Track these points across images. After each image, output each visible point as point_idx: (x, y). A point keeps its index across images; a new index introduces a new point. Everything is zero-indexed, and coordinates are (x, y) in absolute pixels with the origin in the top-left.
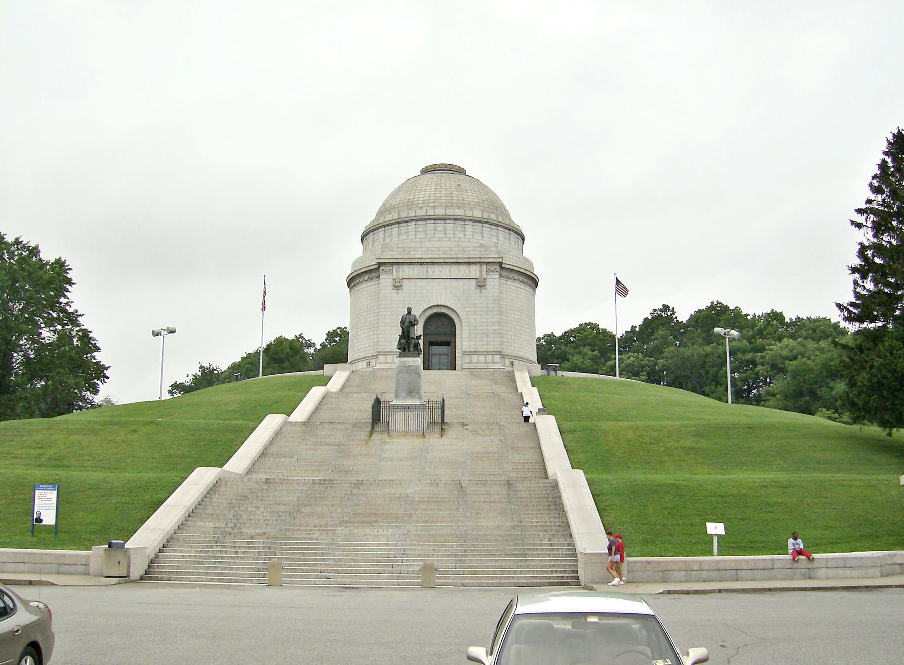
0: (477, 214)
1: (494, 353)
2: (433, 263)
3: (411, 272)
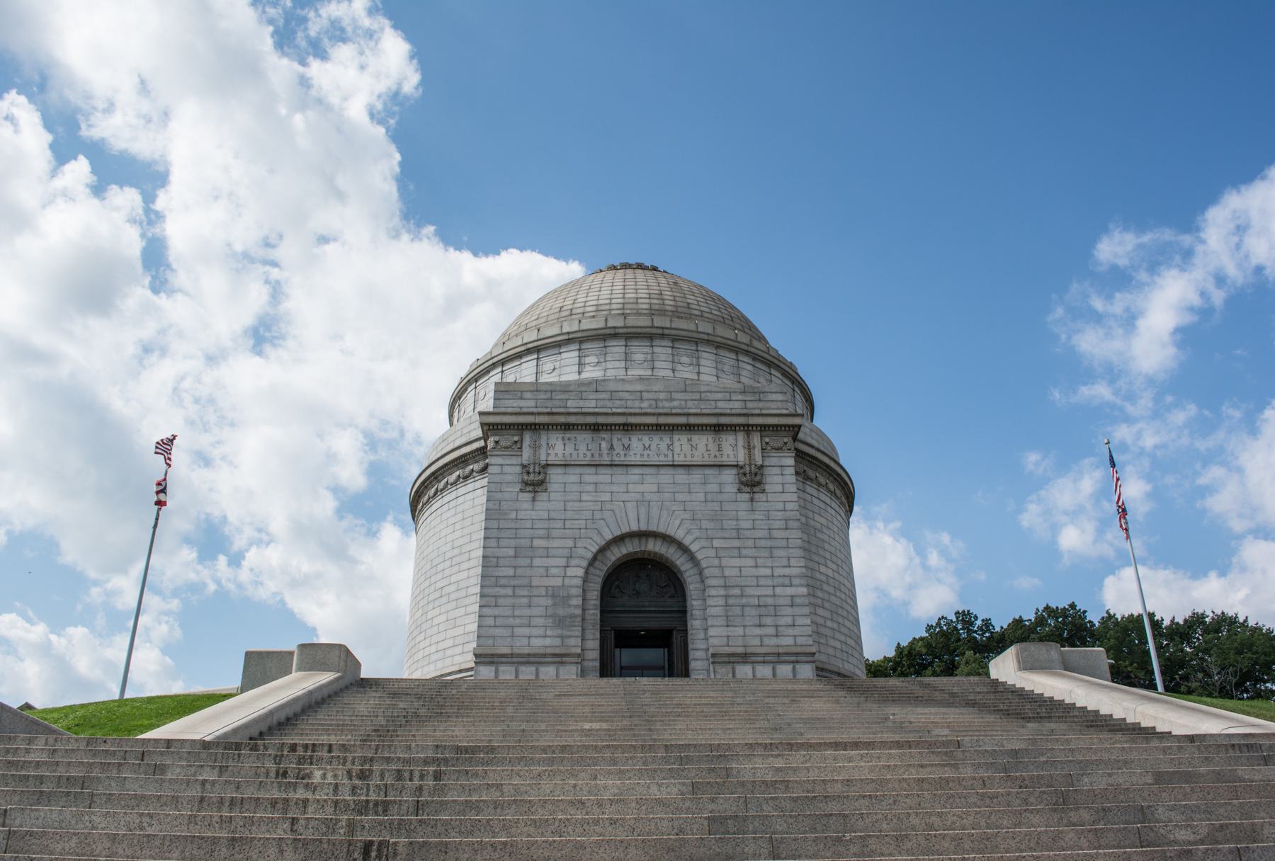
1: (795, 657)
2: (627, 428)
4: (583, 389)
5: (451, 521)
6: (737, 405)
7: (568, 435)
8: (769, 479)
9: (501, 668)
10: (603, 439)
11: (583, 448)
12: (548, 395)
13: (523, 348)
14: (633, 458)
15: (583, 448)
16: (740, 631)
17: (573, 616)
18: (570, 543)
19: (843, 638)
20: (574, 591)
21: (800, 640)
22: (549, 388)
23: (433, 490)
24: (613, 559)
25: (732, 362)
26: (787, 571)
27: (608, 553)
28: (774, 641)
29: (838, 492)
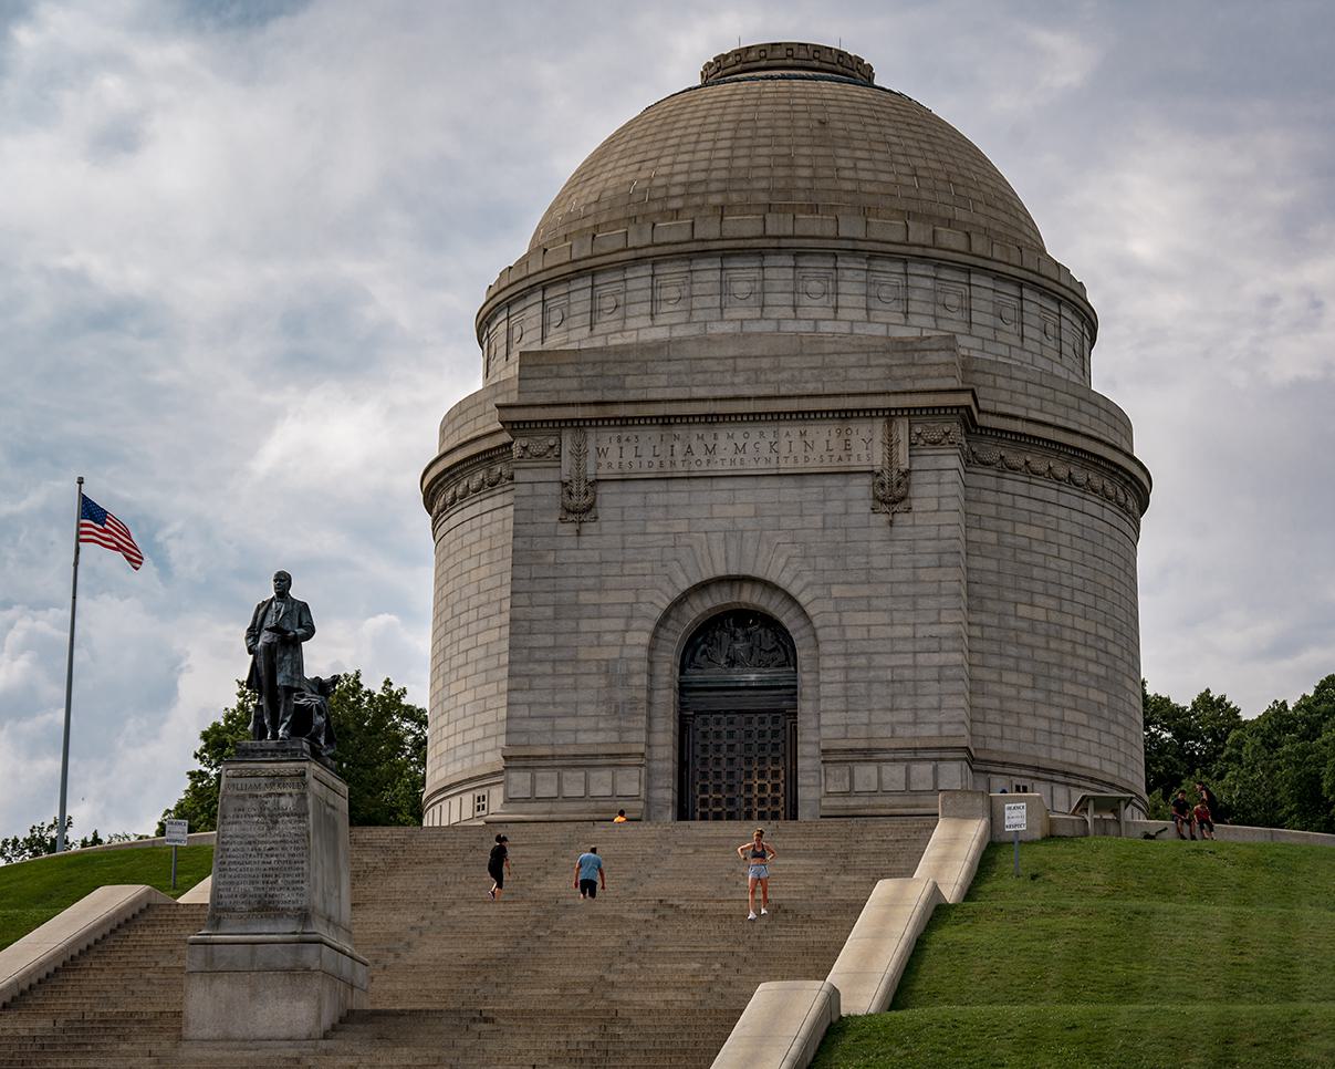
0: (889, 230)
1: (937, 753)
2: (711, 420)
3: (629, 454)
4: (648, 356)
5: (476, 549)
6: (877, 373)
7: (626, 433)
8: (916, 491)
9: (540, 774)
10: (677, 438)
11: (647, 455)
12: (598, 370)
13: (569, 269)
14: (720, 467)
15: (647, 455)
16: (863, 717)
17: (634, 701)
18: (629, 597)
19: (1056, 713)
20: (635, 666)
21: (947, 729)
22: (599, 358)
23: (449, 494)
24: (694, 615)
25: (895, 279)
26: (935, 630)
27: (686, 608)
28: (909, 731)
29: (1080, 476)
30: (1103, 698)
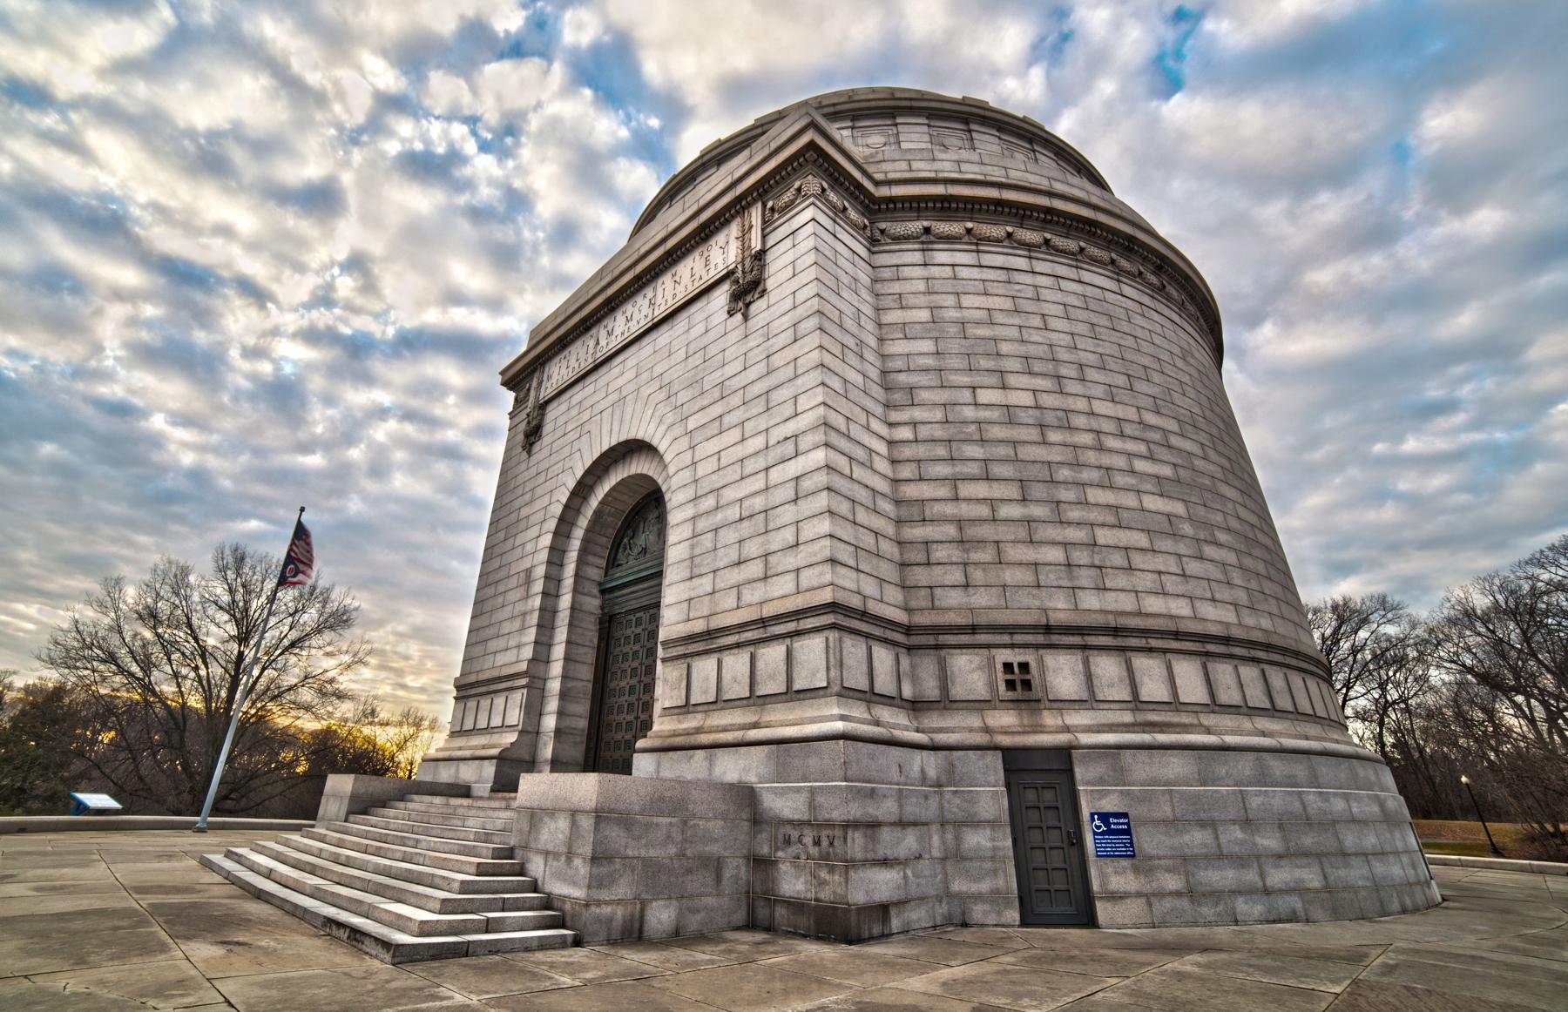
28: (752, 595)
30: (1179, 508)
